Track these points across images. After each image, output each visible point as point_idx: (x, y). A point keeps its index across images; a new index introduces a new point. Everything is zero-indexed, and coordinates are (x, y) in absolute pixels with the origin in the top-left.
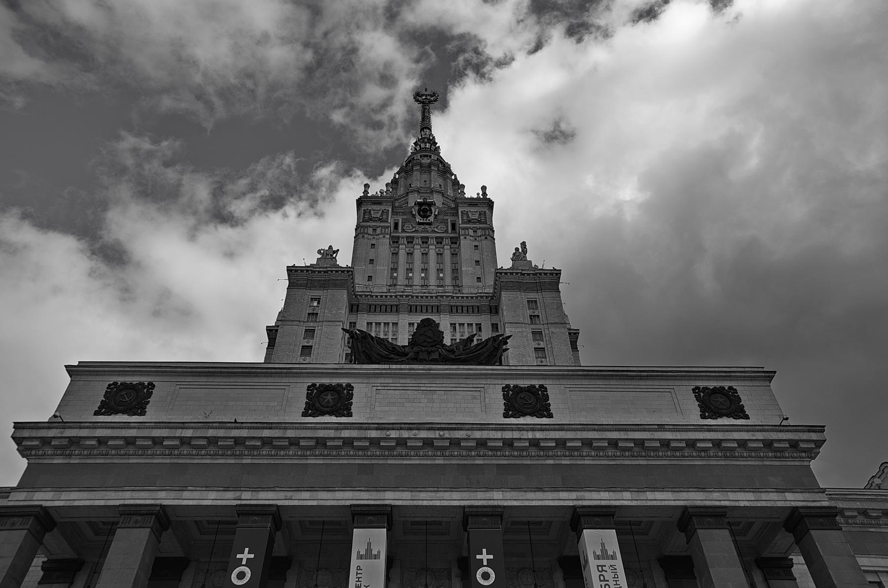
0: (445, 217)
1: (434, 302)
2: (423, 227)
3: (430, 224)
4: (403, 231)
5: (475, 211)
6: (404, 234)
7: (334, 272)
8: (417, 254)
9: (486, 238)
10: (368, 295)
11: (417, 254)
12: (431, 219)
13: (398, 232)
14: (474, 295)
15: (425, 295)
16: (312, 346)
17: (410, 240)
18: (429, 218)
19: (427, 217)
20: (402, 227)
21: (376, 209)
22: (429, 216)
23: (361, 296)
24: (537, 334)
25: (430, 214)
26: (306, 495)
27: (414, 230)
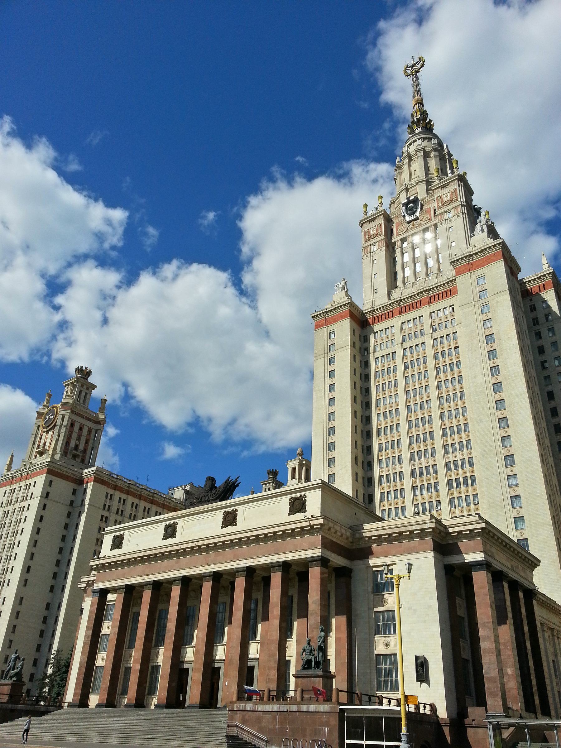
0: (428, 207)
1: (417, 299)
2: (411, 224)
3: (417, 219)
4: (398, 234)
9: (458, 216)
10: (371, 311)
12: (417, 214)
14: (445, 282)
15: (409, 295)
18: (415, 214)
19: (413, 213)
20: (397, 231)
22: (416, 211)
23: (367, 313)
26: (161, 575)
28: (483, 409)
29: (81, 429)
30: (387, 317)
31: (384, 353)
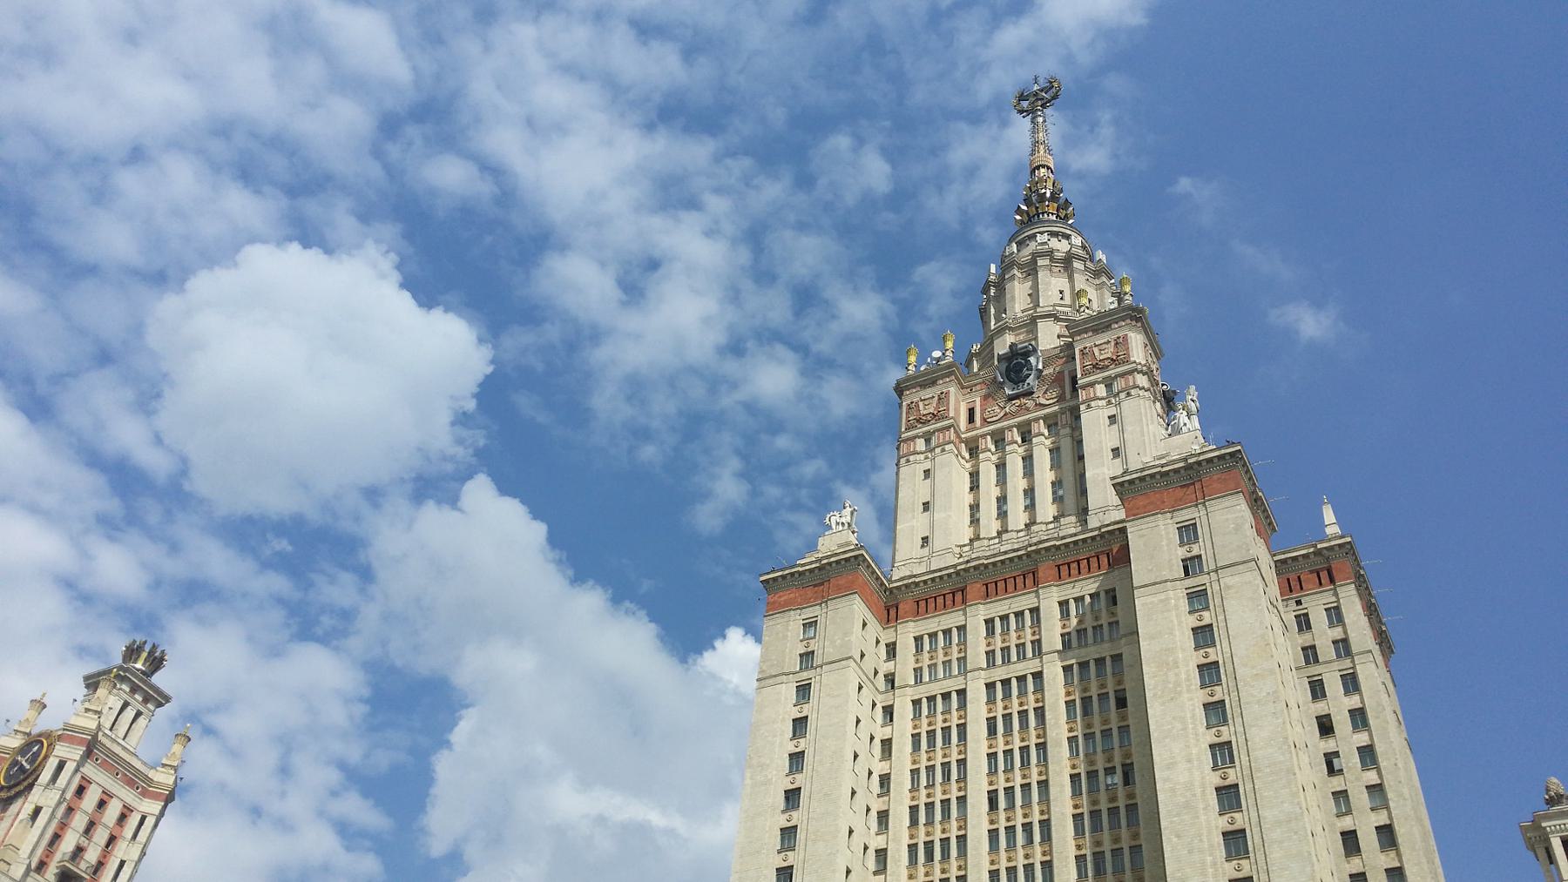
2: (1017, 402)
3: (1029, 393)
5: (1105, 340)
6: (986, 429)
7: (834, 565)
8: (1015, 465)
9: (1129, 394)
11: (1015, 465)
13: (976, 429)
16: (807, 717)
17: (999, 440)
18: (1027, 382)
20: (982, 414)
21: (927, 397)
24: (1198, 598)
25: (1029, 372)
27: (1002, 414)
28: (1190, 852)
29: (102, 804)
30: (949, 602)
31: (937, 689)
